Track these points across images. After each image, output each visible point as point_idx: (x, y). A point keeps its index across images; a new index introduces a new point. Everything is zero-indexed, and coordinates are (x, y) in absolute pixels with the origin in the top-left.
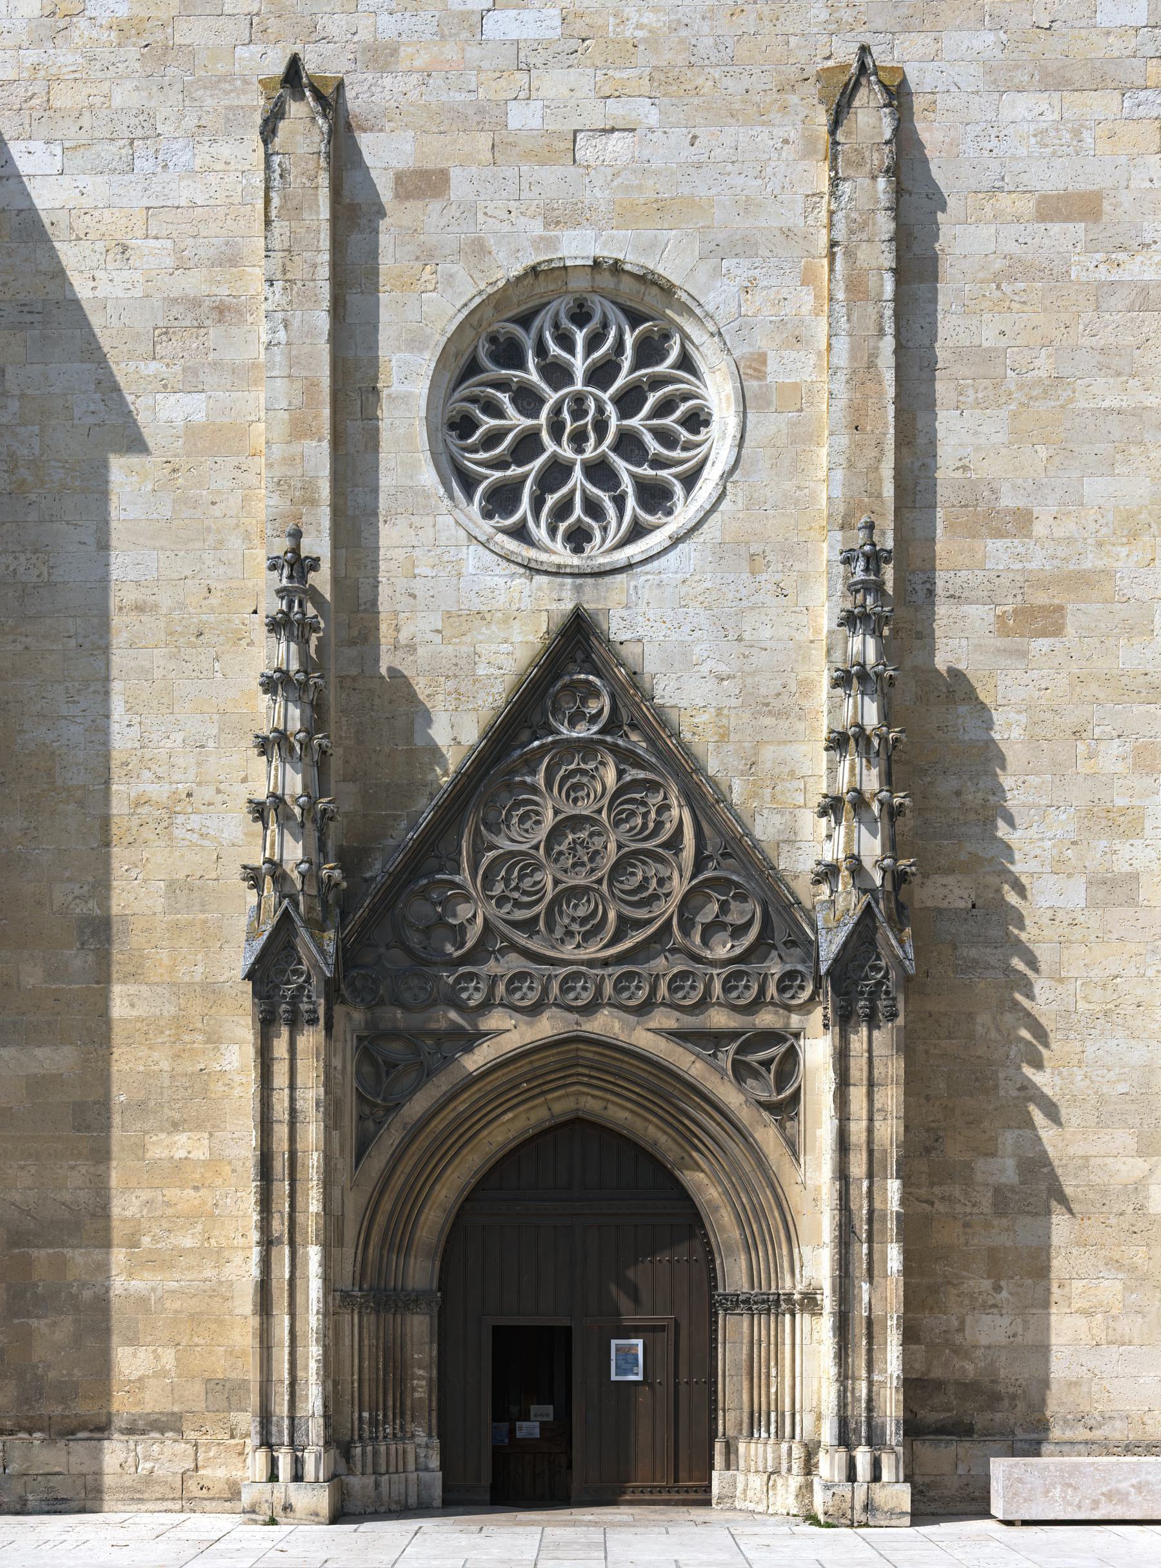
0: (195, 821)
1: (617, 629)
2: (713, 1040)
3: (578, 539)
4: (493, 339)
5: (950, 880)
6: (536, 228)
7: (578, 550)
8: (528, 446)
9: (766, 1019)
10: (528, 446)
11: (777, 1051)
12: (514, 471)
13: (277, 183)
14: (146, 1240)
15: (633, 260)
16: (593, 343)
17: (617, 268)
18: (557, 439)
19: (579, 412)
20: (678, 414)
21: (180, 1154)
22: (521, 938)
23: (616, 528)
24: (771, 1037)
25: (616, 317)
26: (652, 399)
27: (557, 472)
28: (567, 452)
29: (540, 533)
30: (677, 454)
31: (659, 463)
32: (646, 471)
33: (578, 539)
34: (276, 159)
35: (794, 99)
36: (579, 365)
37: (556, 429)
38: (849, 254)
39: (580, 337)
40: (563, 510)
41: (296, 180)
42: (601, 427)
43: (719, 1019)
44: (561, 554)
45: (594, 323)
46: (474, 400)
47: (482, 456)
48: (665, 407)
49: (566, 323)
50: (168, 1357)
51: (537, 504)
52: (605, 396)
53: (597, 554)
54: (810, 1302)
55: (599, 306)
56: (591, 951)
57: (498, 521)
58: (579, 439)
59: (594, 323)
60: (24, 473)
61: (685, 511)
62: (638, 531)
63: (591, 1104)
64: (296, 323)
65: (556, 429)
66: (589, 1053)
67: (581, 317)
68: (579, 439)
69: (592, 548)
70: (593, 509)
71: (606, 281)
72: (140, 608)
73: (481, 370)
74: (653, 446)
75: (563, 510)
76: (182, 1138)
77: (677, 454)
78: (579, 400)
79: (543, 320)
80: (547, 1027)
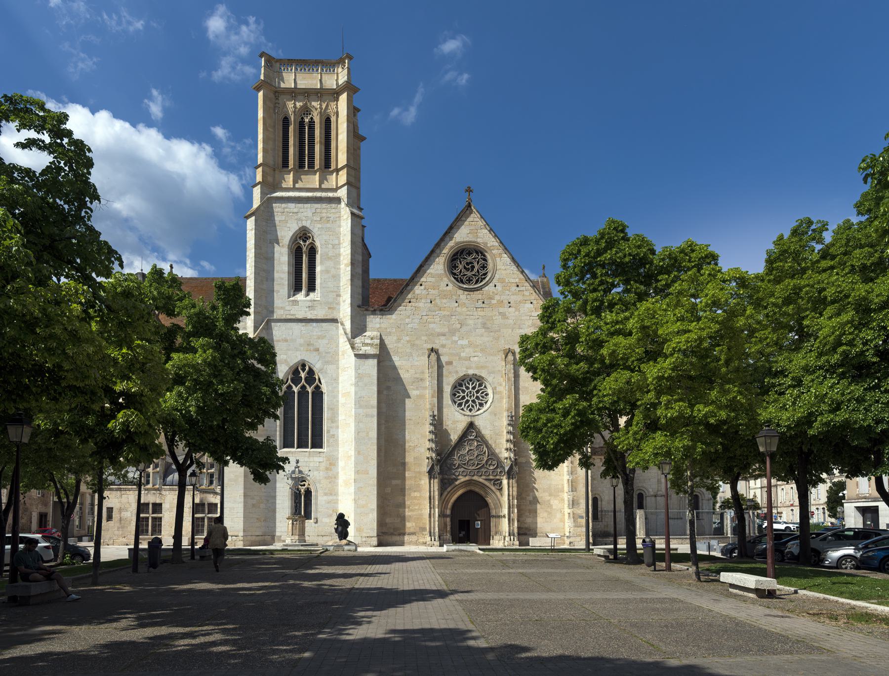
3: (470, 410)
15: (478, 374)
16: (472, 384)
23: (476, 409)
27: (467, 401)
33: (470, 410)
40: (469, 406)
41: (432, 363)
44: (468, 413)
48: (482, 393)
53: (473, 413)
55: (473, 379)
58: (470, 397)
61: (486, 407)
62: (479, 409)
65: (467, 395)
68: (470, 397)
75: (469, 406)
79: (466, 381)
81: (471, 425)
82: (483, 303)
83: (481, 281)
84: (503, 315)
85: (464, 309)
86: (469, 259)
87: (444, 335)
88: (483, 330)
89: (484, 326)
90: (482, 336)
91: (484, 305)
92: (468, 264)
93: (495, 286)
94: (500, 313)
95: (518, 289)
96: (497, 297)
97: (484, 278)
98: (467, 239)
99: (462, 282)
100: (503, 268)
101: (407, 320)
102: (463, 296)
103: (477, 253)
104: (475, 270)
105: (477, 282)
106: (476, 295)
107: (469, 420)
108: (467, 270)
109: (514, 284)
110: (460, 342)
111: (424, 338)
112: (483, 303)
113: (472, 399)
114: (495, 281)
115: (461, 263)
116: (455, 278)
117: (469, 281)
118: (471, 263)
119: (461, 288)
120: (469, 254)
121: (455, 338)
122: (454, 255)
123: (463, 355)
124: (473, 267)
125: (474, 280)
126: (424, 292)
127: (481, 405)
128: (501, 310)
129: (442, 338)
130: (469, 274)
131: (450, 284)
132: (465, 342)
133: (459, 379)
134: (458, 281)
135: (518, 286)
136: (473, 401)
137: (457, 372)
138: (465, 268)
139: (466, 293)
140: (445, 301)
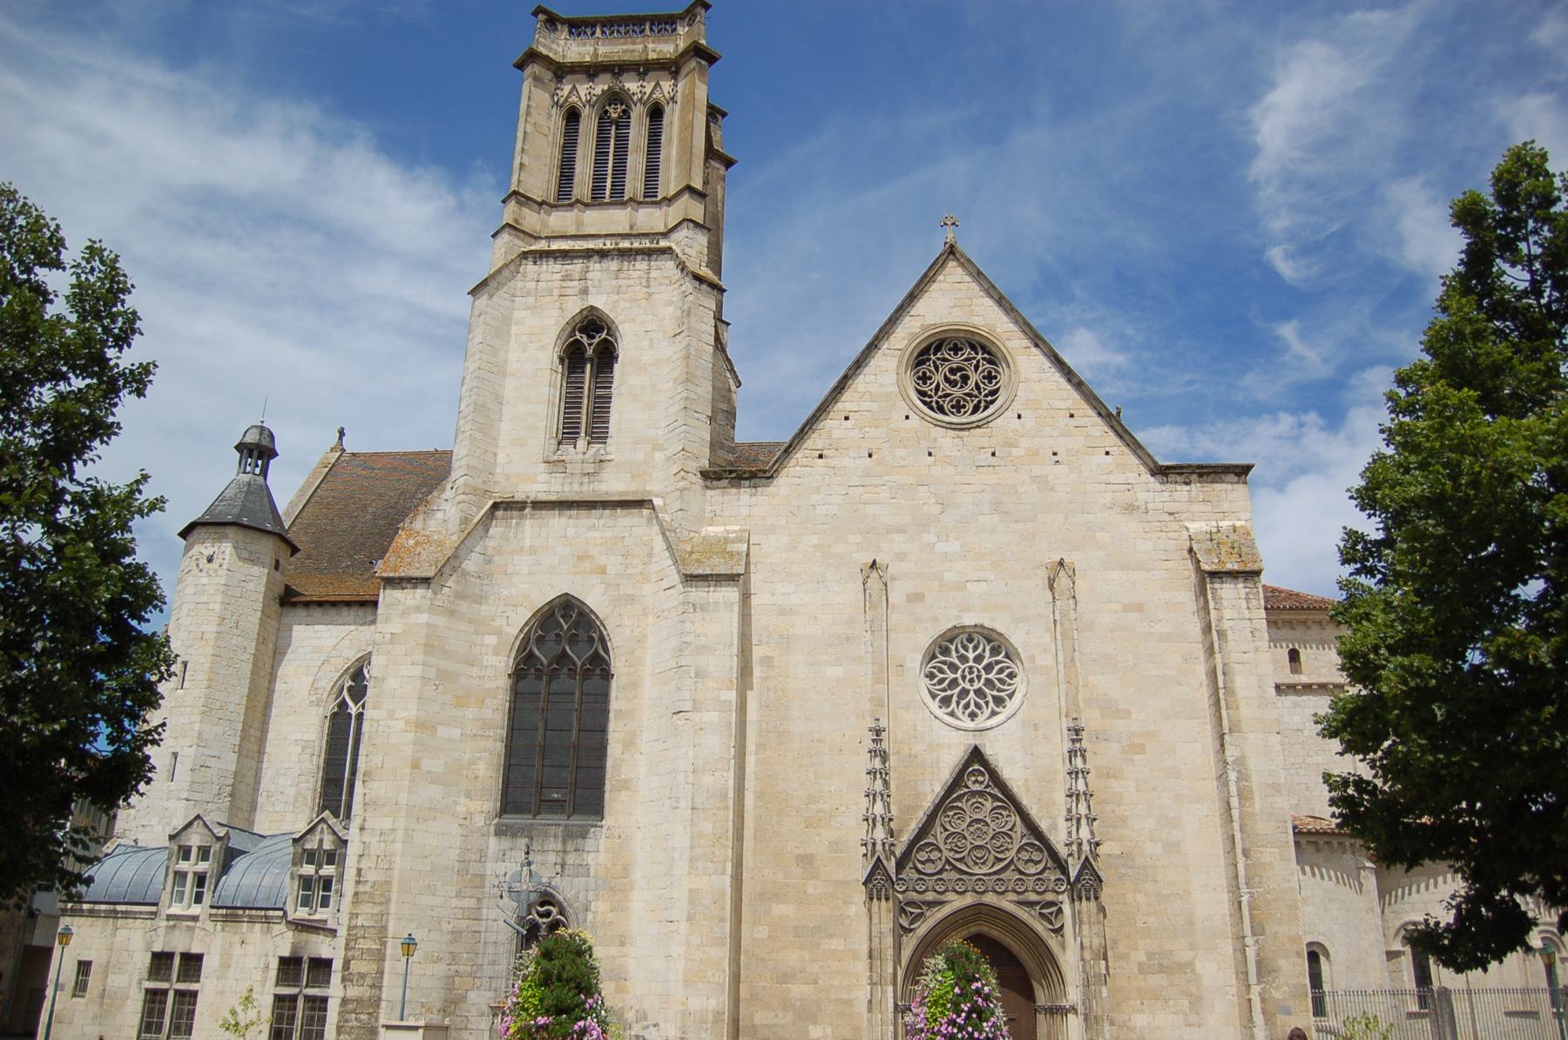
0: (839, 819)
1: (988, 751)
2: (1031, 904)
3: (973, 716)
4: (940, 647)
5: (1113, 843)
6: (955, 612)
7: (973, 720)
8: (954, 683)
9: (1050, 897)
10: (954, 683)
11: (1054, 909)
12: (949, 693)
13: (868, 598)
14: (820, 982)
15: (987, 624)
16: (975, 648)
17: (982, 627)
18: (964, 681)
19: (971, 673)
20: (1005, 673)
21: (833, 947)
22: (958, 865)
23: (987, 712)
24: (1052, 904)
25: (983, 641)
26: (997, 668)
27: (964, 692)
28: (967, 686)
29: (959, 713)
30: (1006, 687)
31: (1000, 690)
32: (995, 693)
33: (973, 716)
34: (867, 592)
35: (1039, 572)
36: (971, 655)
37: (964, 677)
38: (1061, 624)
39: (971, 646)
40: (967, 706)
41: (874, 598)
42: (979, 677)
43: (1033, 897)
44: (969, 724)
45: (975, 642)
46: (934, 668)
47: (938, 687)
48: (1001, 671)
49: (965, 642)
50: (829, 1030)
51: (958, 703)
52: (980, 667)
53: (981, 722)
54: (1074, 1009)
55: (976, 637)
56: (985, 870)
57: (944, 710)
58: (971, 681)
59: (975, 642)
60: (779, 693)
61: (1011, 705)
62: (994, 713)
63: (985, 929)
64: (875, 645)
65: (964, 677)
66: (984, 910)
67: (970, 640)
68: (971, 681)
69: (977, 720)
70: (978, 706)
71: (978, 630)
72: (820, 741)
73: (937, 657)
74: (998, 685)
75: (967, 706)
76: (834, 941)
77: (1006, 687)
78: (971, 668)
79: (958, 641)
80: (969, 899)
81: (976, 755)
82: (993, 454)
83: (986, 408)
84: (1043, 483)
85: (949, 470)
86: (956, 361)
87: (902, 531)
88: (996, 518)
89: (997, 507)
90: (994, 531)
91: (994, 461)
92: (953, 372)
93: (1019, 417)
94: (1034, 478)
95: (1072, 422)
96: (1025, 443)
97: (992, 402)
98: (950, 319)
99: (941, 410)
100: (1035, 377)
101: (814, 498)
102: (946, 441)
103: (973, 348)
104: (971, 383)
105: (976, 409)
106: (977, 437)
107: (971, 740)
108: (953, 384)
109: (1062, 412)
110: (941, 547)
111: (854, 539)
112: (993, 454)
113: (976, 686)
114: (1017, 407)
115: (937, 368)
116: (925, 403)
117: (958, 407)
118: (960, 369)
119: (938, 424)
120: (956, 349)
121: (930, 538)
122: (922, 353)
123: (949, 577)
124: (965, 379)
125: (970, 407)
126: (856, 434)
127: (999, 701)
128: (1037, 470)
129: (897, 537)
130: (957, 392)
131: (912, 415)
132: (953, 546)
133: (942, 636)
134: (932, 408)
135: (1072, 416)
136: (979, 692)
137: (936, 619)
138: (947, 379)
139: (952, 433)
140: (901, 452)
